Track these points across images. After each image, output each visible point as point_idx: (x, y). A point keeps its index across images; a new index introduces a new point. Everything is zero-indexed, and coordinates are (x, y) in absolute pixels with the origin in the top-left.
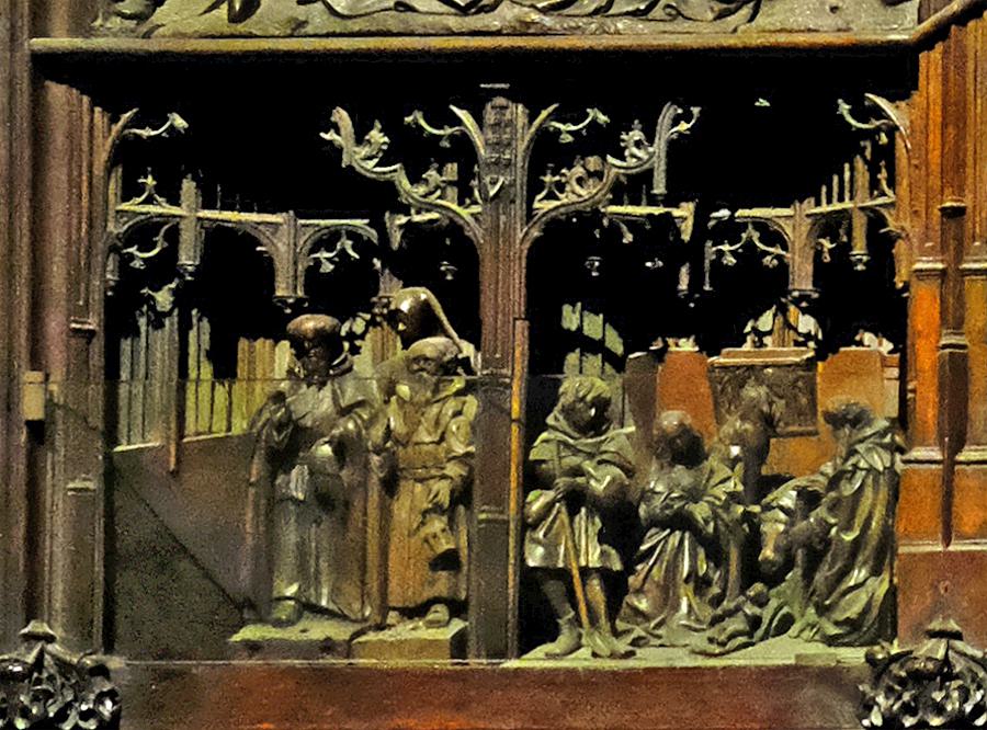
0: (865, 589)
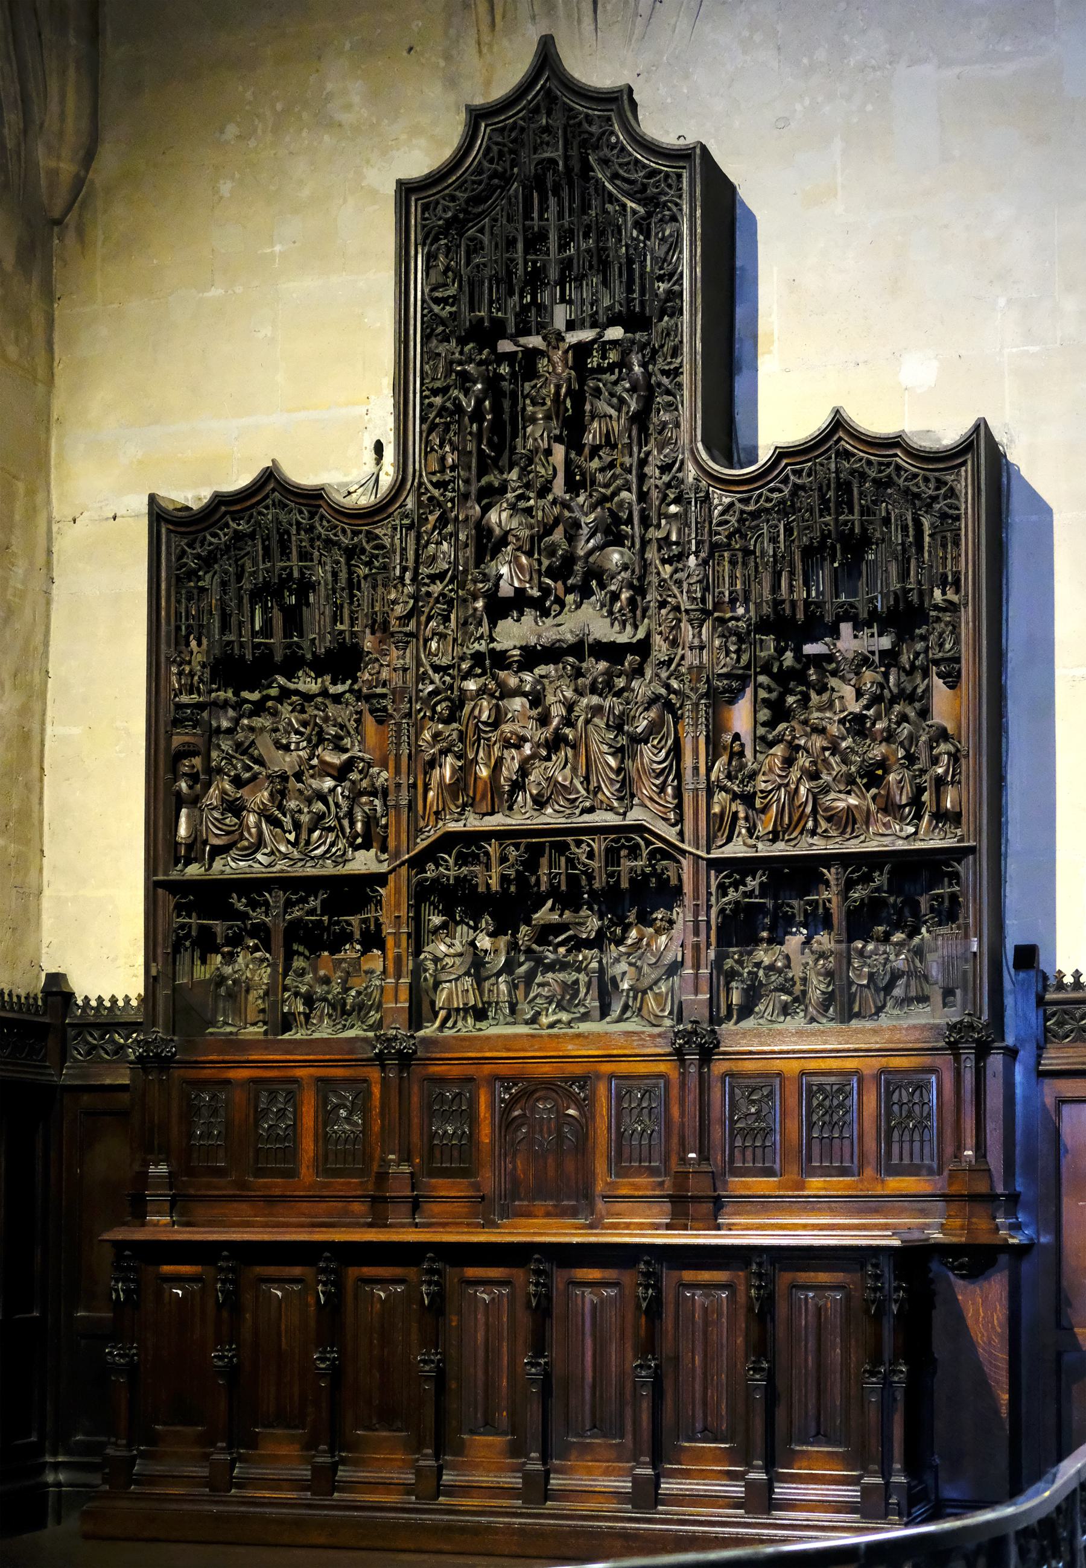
0: (374, 1016)
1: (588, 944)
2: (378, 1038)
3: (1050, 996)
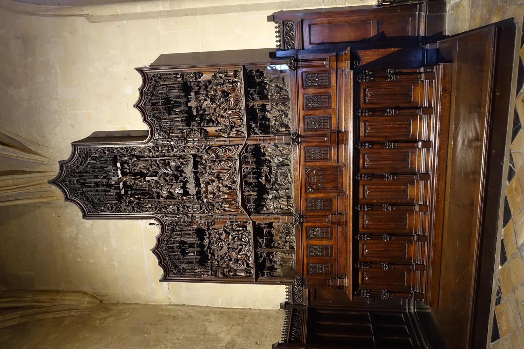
0: (290, 225)
1: (270, 170)
2: (295, 224)
3: (282, 48)
